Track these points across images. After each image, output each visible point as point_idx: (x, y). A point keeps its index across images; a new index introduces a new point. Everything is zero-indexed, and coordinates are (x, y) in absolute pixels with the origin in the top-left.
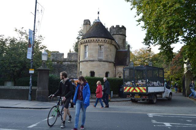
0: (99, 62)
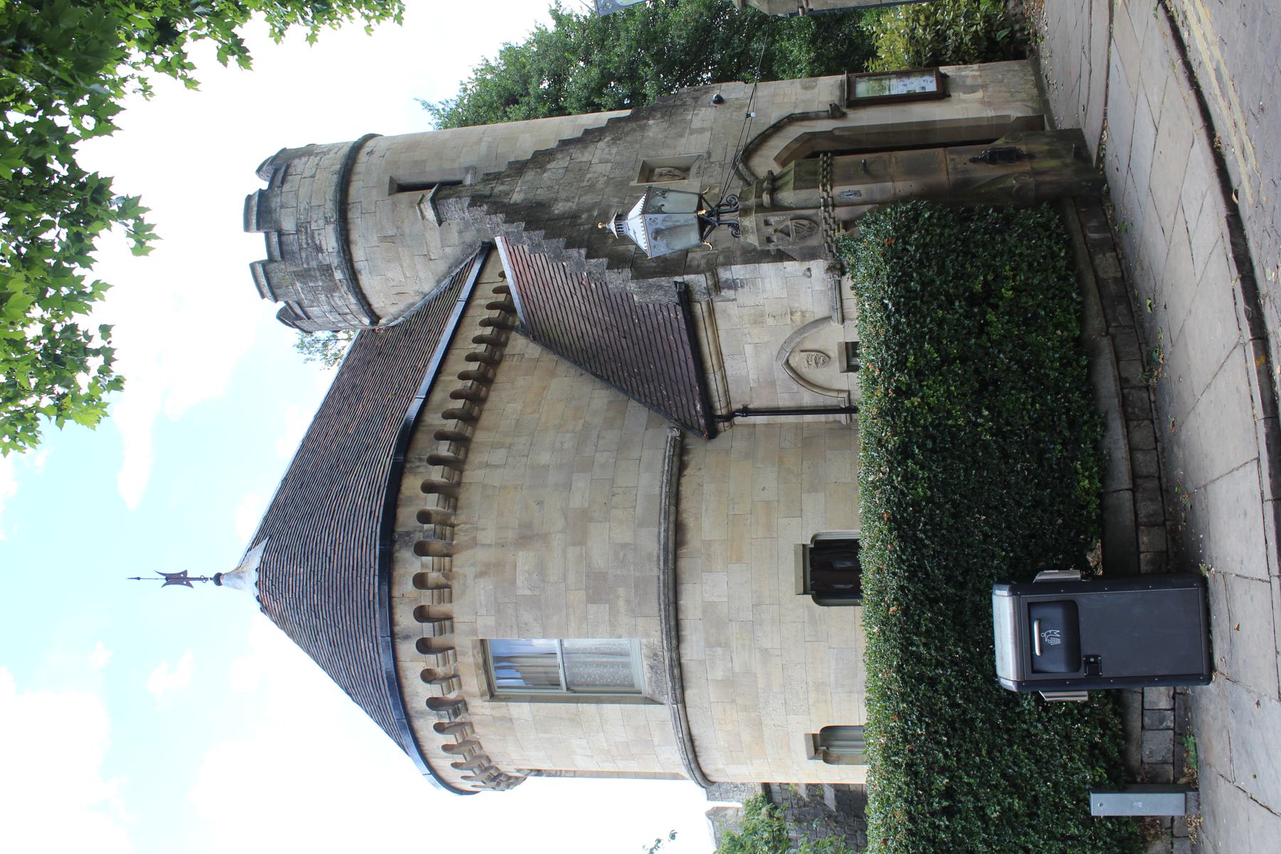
0: (689, 694)
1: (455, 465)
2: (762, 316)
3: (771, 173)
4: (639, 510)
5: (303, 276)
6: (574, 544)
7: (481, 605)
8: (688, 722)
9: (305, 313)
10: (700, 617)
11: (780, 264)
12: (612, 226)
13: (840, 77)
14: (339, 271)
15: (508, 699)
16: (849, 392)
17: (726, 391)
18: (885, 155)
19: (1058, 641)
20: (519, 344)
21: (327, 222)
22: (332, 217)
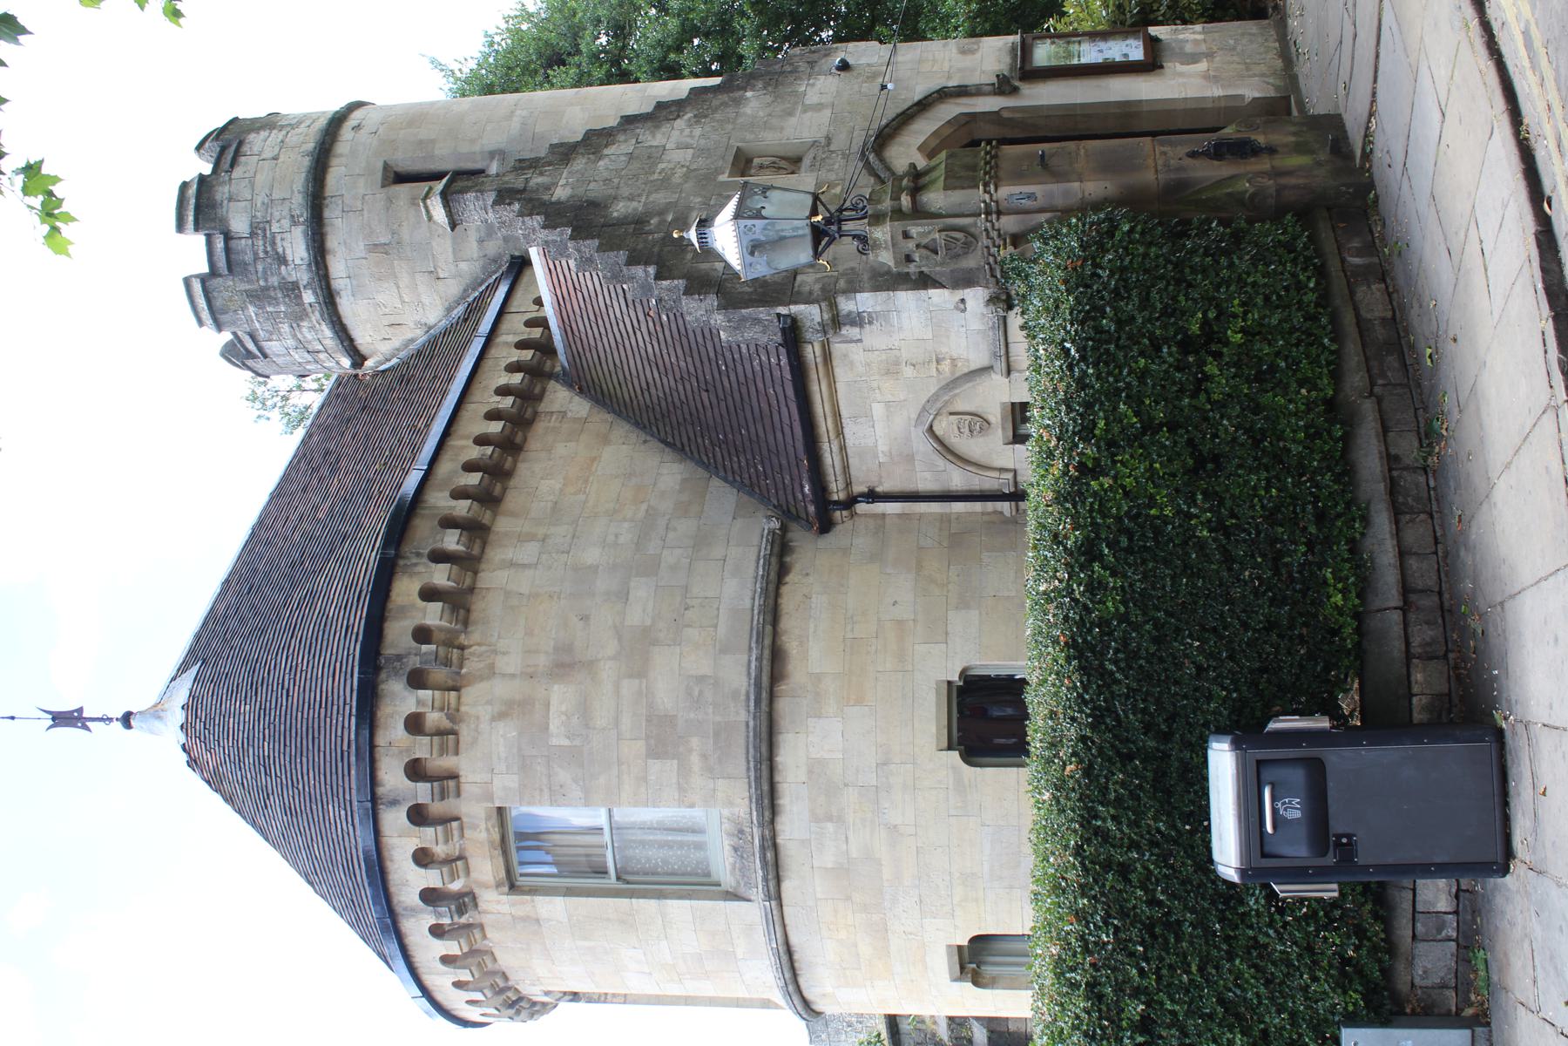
0: (787, 886)
1: (467, 563)
2: (897, 363)
3: (913, 166)
4: (722, 630)
5: (258, 297)
6: (631, 676)
7: (499, 758)
8: (784, 926)
9: (260, 349)
10: (804, 779)
11: (923, 293)
12: (692, 235)
13: (1011, 39)
14: (310, 292)
15: (533, 891)
16: (1015, 471)
17: (846, 468)
18: (1071, 145)
19: (1297, 814)
20: (559, 397)
21: (294, 223)
22: (302, 216)
